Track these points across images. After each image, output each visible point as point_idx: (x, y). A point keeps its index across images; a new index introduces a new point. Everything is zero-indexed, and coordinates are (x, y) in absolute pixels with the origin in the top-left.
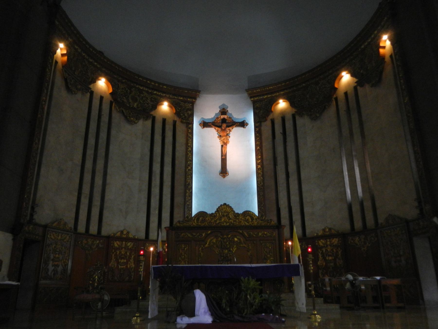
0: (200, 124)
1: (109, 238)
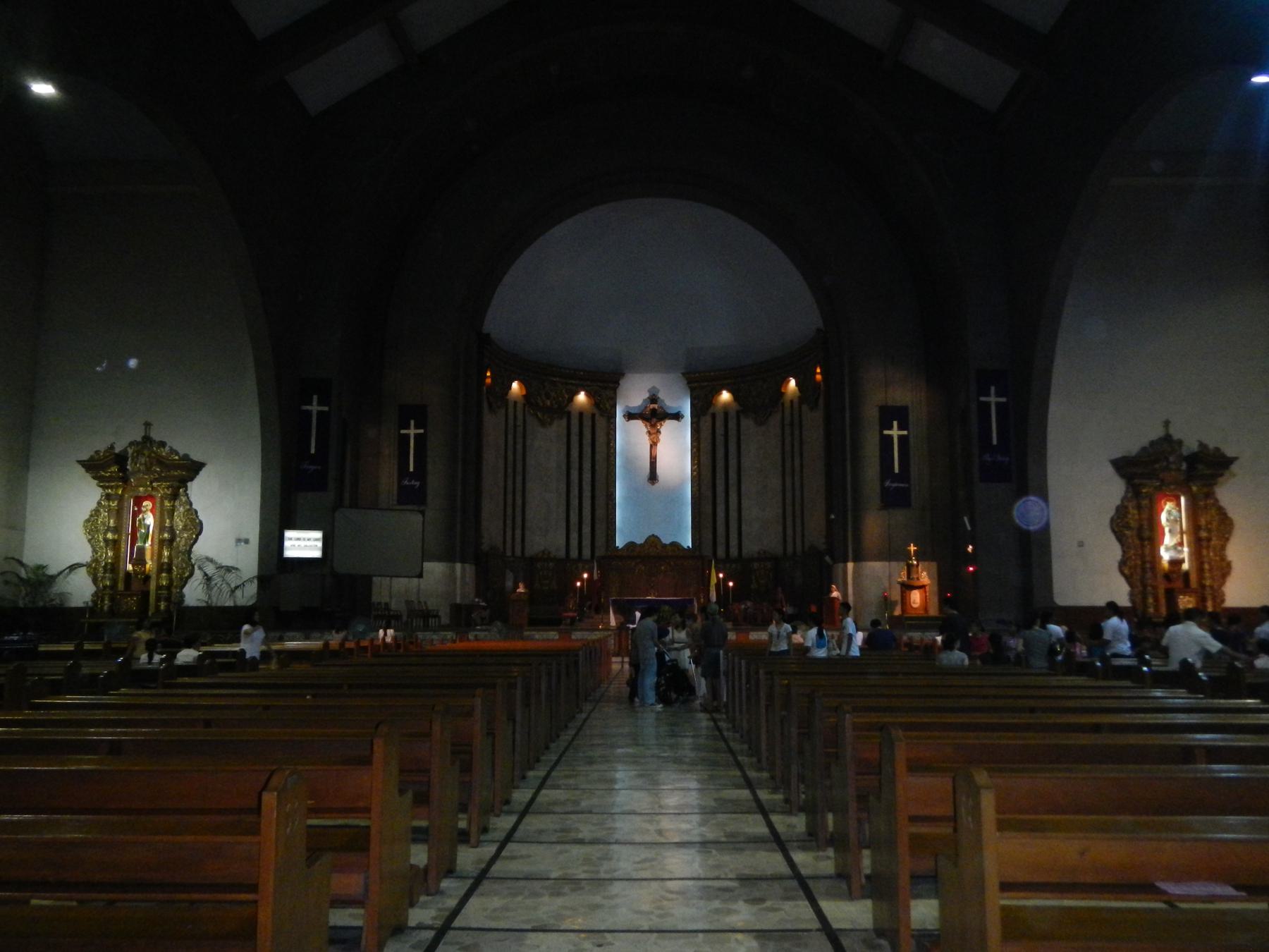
0: (624, 416)
1: (533, 560)
